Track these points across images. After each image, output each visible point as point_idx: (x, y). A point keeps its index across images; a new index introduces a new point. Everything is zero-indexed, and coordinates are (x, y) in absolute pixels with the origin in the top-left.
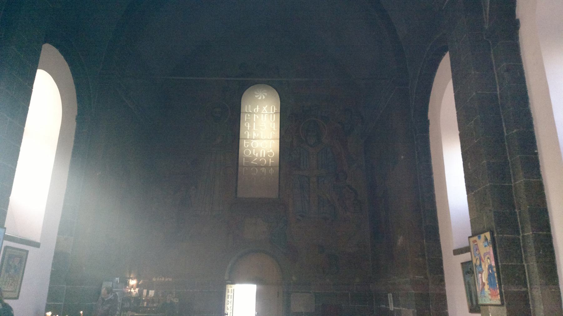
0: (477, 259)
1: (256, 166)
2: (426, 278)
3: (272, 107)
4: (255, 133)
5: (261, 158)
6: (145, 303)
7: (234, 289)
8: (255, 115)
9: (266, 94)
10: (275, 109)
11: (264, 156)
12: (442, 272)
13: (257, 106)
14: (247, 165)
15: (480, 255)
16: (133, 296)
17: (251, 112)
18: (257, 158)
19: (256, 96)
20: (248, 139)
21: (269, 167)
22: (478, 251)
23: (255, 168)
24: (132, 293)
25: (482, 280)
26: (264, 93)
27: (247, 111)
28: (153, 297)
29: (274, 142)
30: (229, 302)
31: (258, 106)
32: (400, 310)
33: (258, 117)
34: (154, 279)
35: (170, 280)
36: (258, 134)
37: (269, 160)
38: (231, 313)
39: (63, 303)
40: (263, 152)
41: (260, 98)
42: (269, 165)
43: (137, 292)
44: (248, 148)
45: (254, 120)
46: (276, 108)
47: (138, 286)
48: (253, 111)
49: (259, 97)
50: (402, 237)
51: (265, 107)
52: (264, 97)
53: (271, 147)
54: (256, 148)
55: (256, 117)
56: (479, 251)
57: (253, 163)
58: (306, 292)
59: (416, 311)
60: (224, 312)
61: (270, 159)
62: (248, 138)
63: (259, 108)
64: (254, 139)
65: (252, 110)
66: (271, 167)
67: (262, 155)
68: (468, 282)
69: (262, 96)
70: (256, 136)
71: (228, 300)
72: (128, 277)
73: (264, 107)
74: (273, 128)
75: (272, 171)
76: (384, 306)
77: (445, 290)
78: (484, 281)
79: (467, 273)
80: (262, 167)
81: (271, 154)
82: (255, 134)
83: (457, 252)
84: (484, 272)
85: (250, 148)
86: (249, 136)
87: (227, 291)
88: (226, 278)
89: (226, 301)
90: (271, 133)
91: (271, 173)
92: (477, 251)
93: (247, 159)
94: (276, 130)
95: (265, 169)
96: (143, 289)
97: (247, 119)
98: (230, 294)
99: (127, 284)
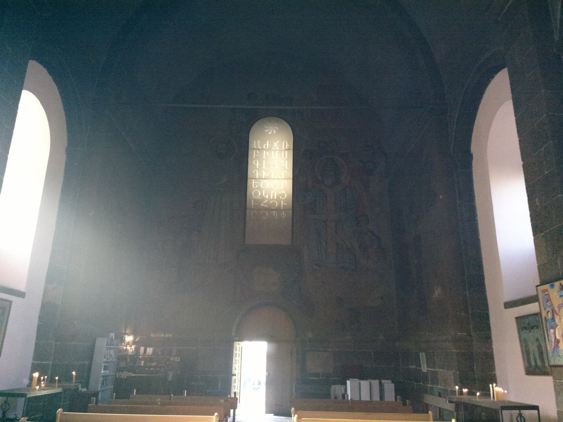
0: (548, 312)
1: (266, 209)
2: (470, 335)
3: (284, 142)
4: (265, 172)
6: (143, 362)
7: (242, 347)
8: (264, 151)
9: (277, 128)
10: (287, 145)
11: (275, 198)
12: (488, 328)
13: (267, 142)
14: (256, 208)
15: (554, 308)
16: (129, 354)
17: (260, 148)
18: (267, 200)
19: (266, 131)
20: (257, 179)
21: (282, 210)
22: (549, 302)
23: (266, 211)
24: (128, 350)
25: (555, 337)
26: (275, 127)
28: (152, 355)
29: (286, 182)
30: (237, 362)
31: (268, 142)
32: (436, 372)
33: (268, 154)
34: (152, 335)
35: (171, 335)
36: (268, 174)
37: (281, 202)
38: (238, 373)
39: (51, 363)
41: (270, 133)
42: (281, 207)
43: (134, 350)
45: (264, 158)
46: (288, 144)
47: (134, 342)
48: (262, 147)
49: (269, 131)
50: (439, 288)
51: (276, 143)
52: (275, 132)
53: (282, 188)
54: (266, 189)
55: (266, 153)
56: (551, 302)
57: (263, 205)
58: (324, 351)
59: (458, 372)
60: (232, 372)
61: (282, 201)
62: (257, 177)
63: (269, 143)
65: (262, 146)
66: (283, 210)
67: (273, 195)
68: (525, 340)
69: (273, 131)
70: (266, 175)
71: (235, 359)
72: (124, 332)
73: (275, 143)
74: (285, 166)
75: (284, 214)
76: (414, 367)
77: (492, 349)
78: (558, 337)
79: (523, 329)
80: (274, 210)
81: (283, 195)
83: (509, 305)
84: (558, 327)
85: (259, 188)
86: (258, 175)
87: (234, 348)
88: (233, 334)
89: (233, 360)
90: (283, 172)
92: (548, 302)
93: (256, 201)
94: (288, 168)
95: (276, 213)
96: (140, 346)
97: (255, 156)
98: (238, 352)
99: (123, 340)
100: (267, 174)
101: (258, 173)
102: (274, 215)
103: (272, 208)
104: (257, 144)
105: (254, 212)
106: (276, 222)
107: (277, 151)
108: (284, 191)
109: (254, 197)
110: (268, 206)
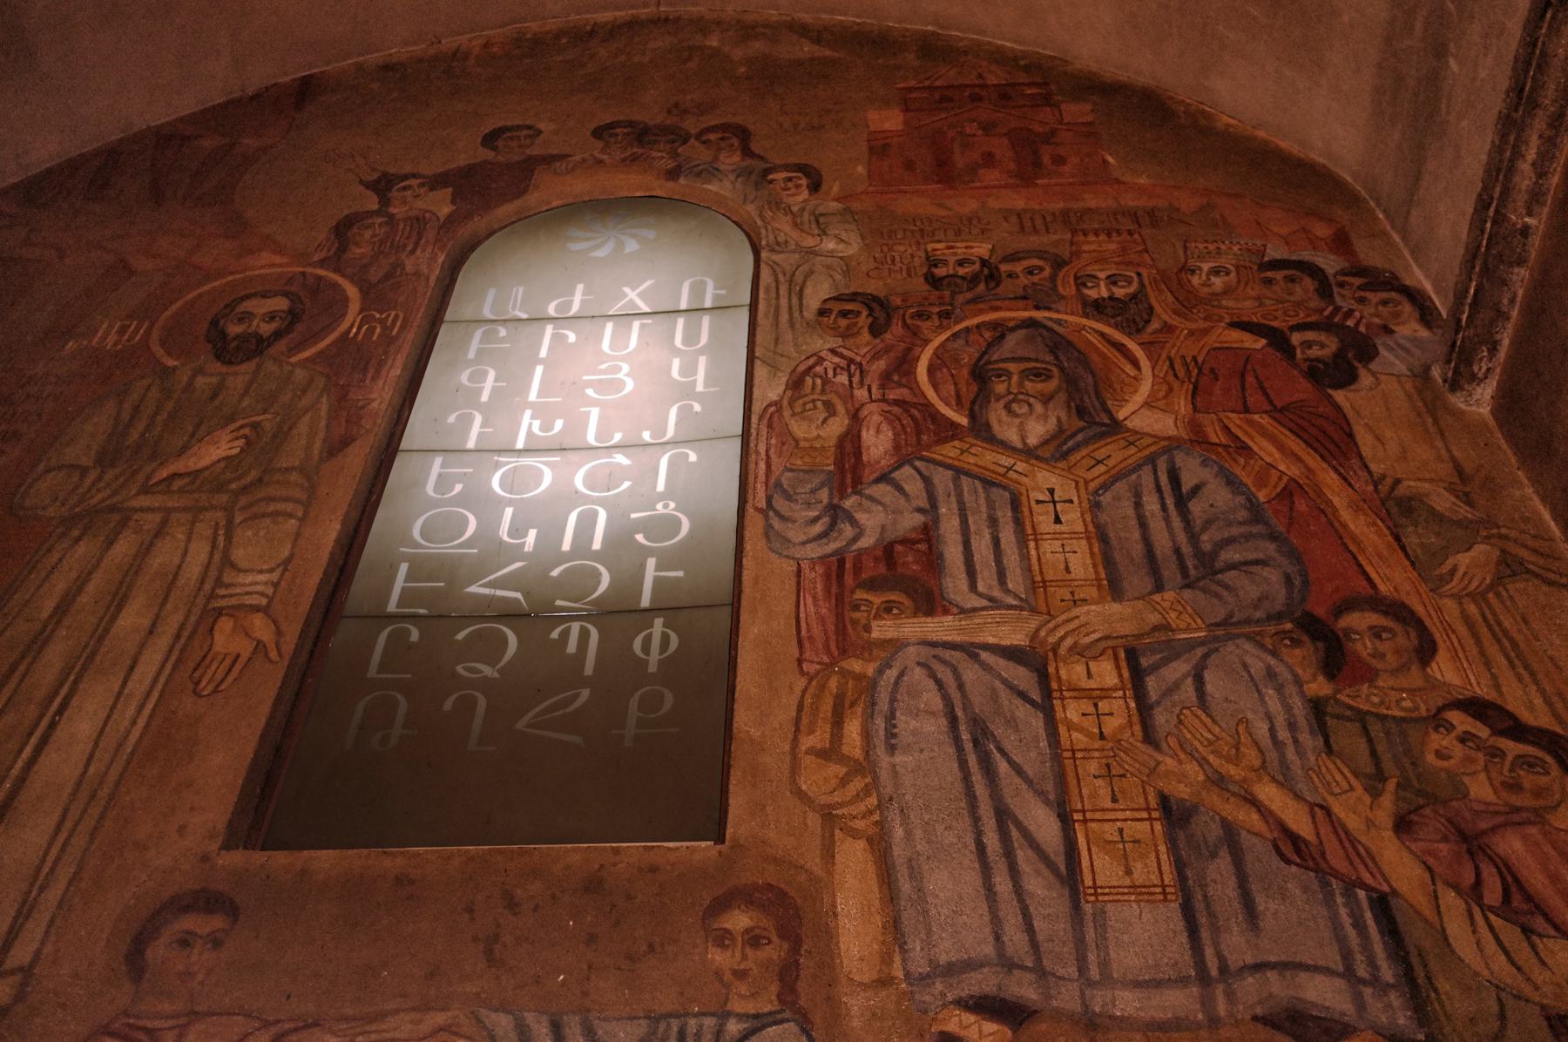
1: (511, 615)
5: (562, 558)
11: (597, 545)
14: (422, 611)
17: (525, 316)
29: (693, 457)
36: (559, 425)
37: (643, 566)
40: (587, 522)
44: (461, 500)
45: (543, 353)
49: (598, 247)
57: (486, 591)
64: (520, 451)
66: (653, 611)
82: (536, 424)
86: (480, 435)
91: (654, 657)
97: (480, 352)
100: (546, 427)
102: (572, 647)
105: (399, 638)
106: (585, 694)
107: (636, 324)
108: (672, 505)
109: (417, 545)
110: (526, 595)
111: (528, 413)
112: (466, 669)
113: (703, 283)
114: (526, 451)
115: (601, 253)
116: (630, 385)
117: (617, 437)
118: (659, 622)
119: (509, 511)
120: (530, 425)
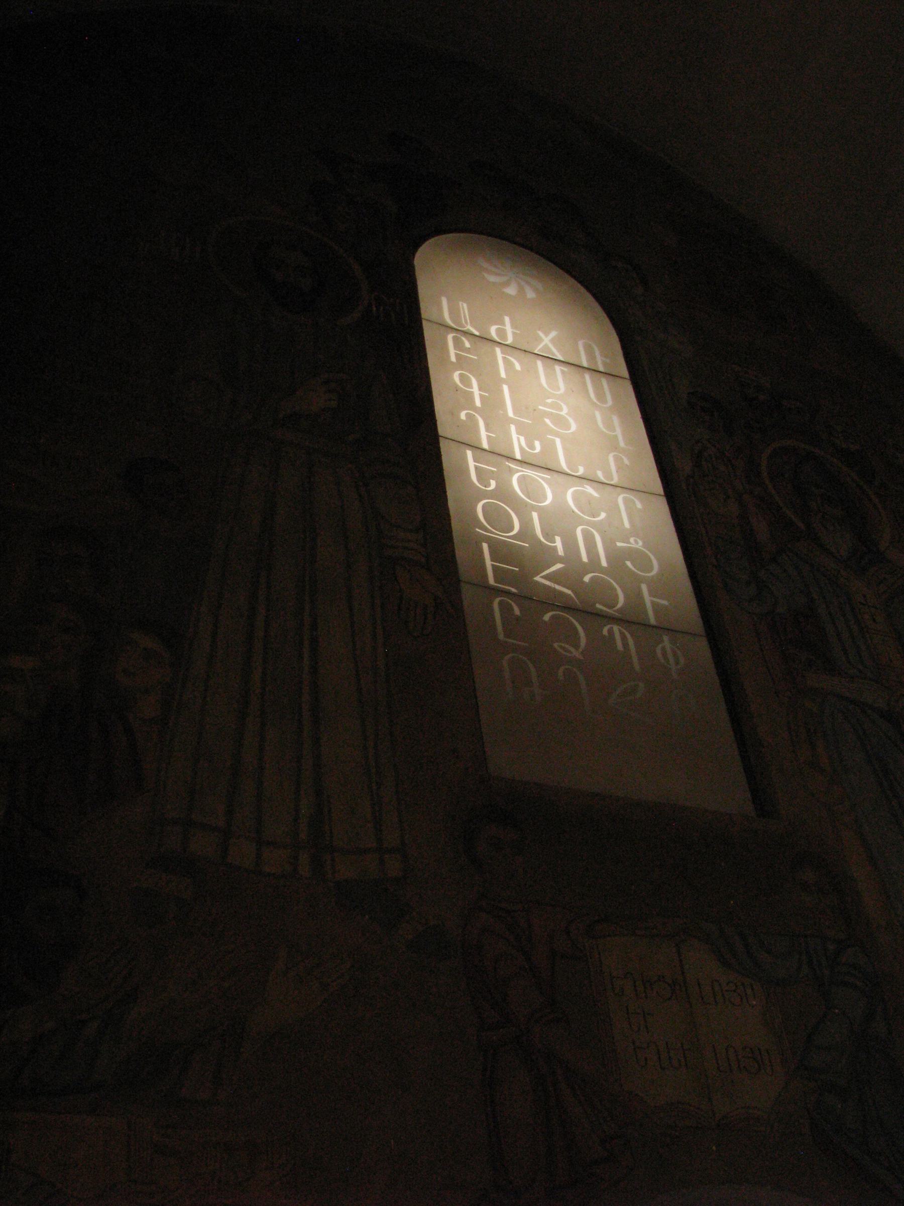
4: (519, 433)
9: (540, 286)
11: (604, 563)
14: (513, 590)
19: (492, 279)
20: (485, 450)
27: (451, 318)
36: (537, 444)
45: (503, 374)
49: (507, 284)
52: (530, 294)
53: (627, 525)
55: (508, 365)
57: (547, 583)
61: (644, 588)
73: (541, 334)
82: (522, 439)
97: (457, 355)
101: (487, 430)
103: (598, 606)
104: (454, 313)
108: (640, 543)
111: (513, 428)
112: (561, 647)
113: (590, 346)
114: (523, 463)
115: (511, 290)
116: (574, 427)
117: (581, 471)
118: (665, 638)
119: (535, 515)
120: (518, 439)
